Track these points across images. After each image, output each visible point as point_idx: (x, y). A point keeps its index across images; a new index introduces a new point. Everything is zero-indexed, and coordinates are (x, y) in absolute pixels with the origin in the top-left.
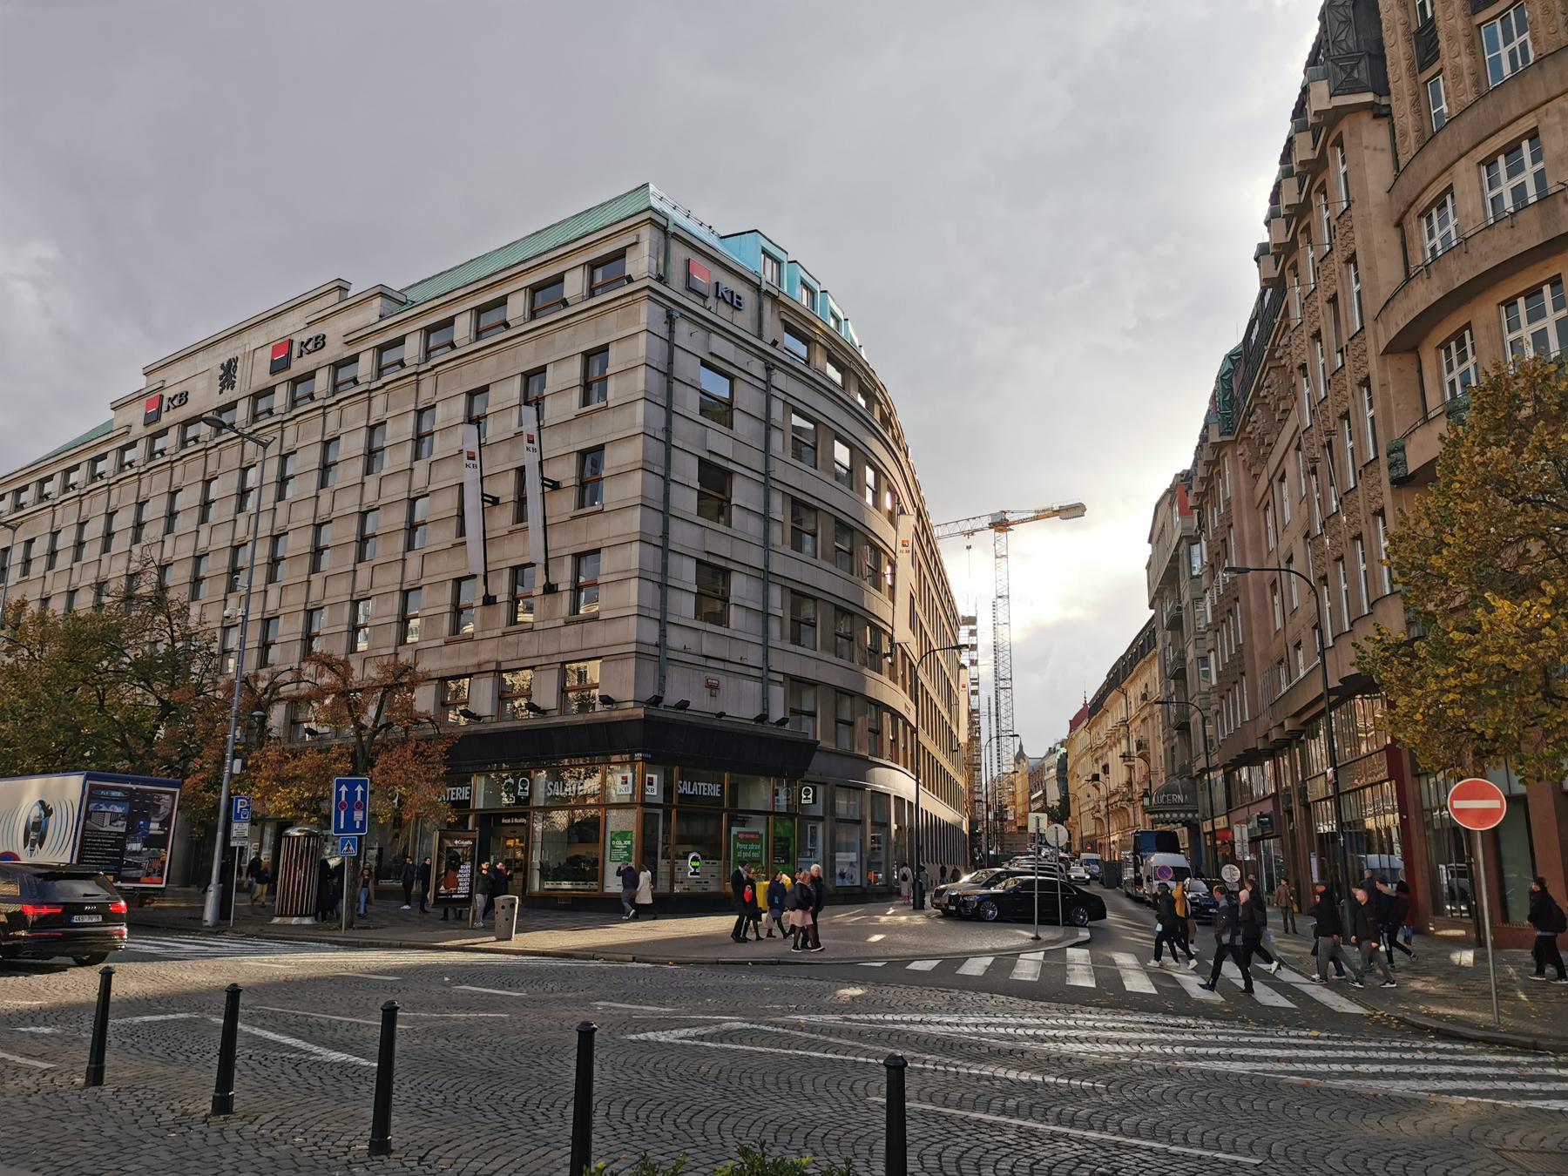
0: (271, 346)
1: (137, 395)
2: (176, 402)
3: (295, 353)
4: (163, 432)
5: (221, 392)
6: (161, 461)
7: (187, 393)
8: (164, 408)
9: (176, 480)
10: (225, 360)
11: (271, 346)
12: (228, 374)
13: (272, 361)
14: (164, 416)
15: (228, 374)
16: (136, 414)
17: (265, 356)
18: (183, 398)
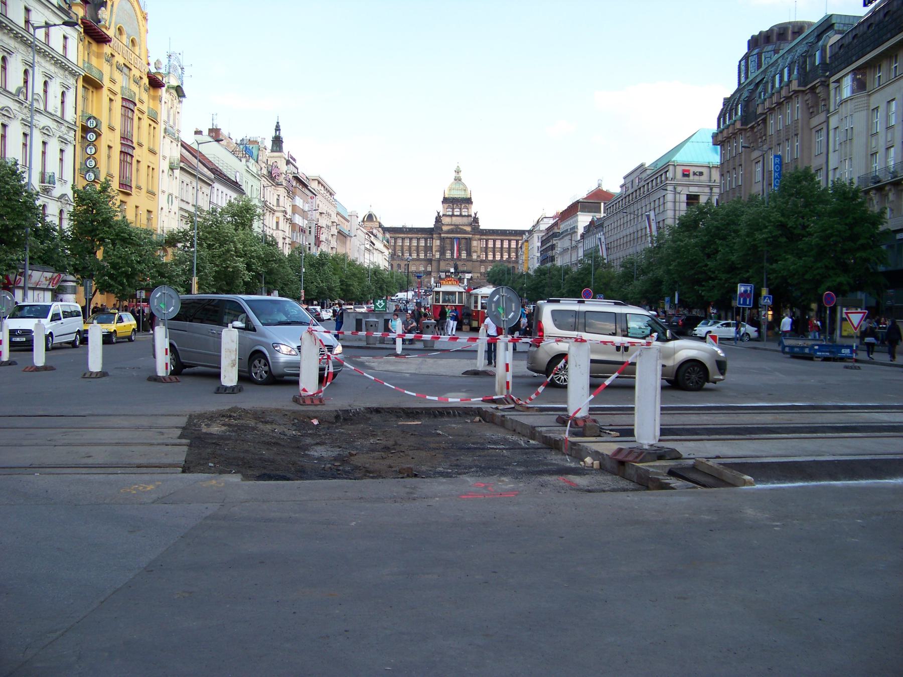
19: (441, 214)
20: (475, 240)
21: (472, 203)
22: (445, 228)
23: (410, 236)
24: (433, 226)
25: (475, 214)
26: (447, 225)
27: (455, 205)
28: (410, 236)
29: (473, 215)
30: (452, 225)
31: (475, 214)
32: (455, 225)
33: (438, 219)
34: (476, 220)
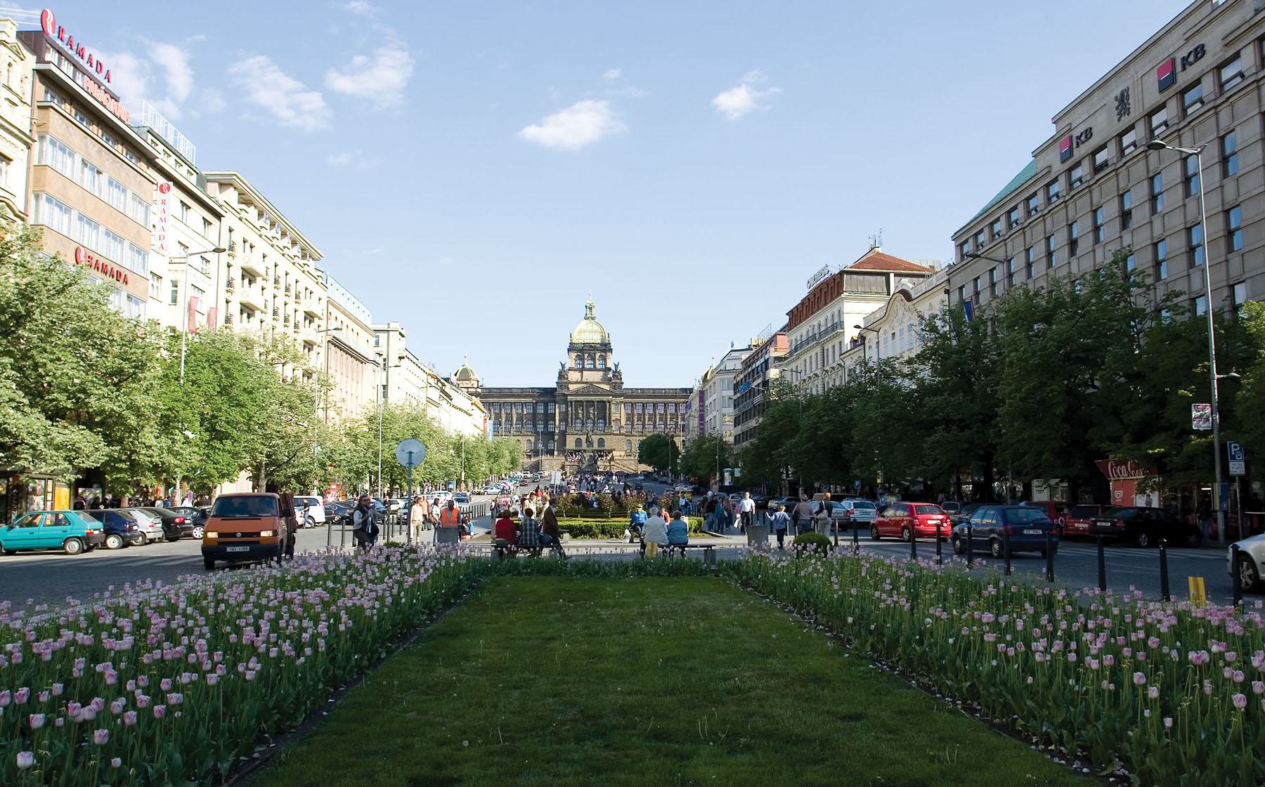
0: (1156, 69)
1: (1051, 141)
2: (1083, 138)
3: (1179, 68)
4: (1078, 164)
5: (1119, 120)
6: (1080, 189)
7: (1091, 129)
8: (1075, 145)
9: (1095, 200)
10: (1117, 93)
11: (1156, 69)
12: (1123, 101)
13: (1160, 82)
14: (1076, 152)
15: (1123, 103)
16: (1053, 159)
17: (1152, 82)
18: (1088, 133)
19: (567, 367)
20: (617, 404)
21: (611, 350)
22: (572, 387)
23: (523, 400)
24: (555, 386)
25: (616, 366)
26: (576, 383)
27: (586, 355)
28: (523, 400)
29: (613, 368)
30: (583, 383)
31: (616, 366)
32: (586, 383)
33: (562, 375)
34: (617, 374)
